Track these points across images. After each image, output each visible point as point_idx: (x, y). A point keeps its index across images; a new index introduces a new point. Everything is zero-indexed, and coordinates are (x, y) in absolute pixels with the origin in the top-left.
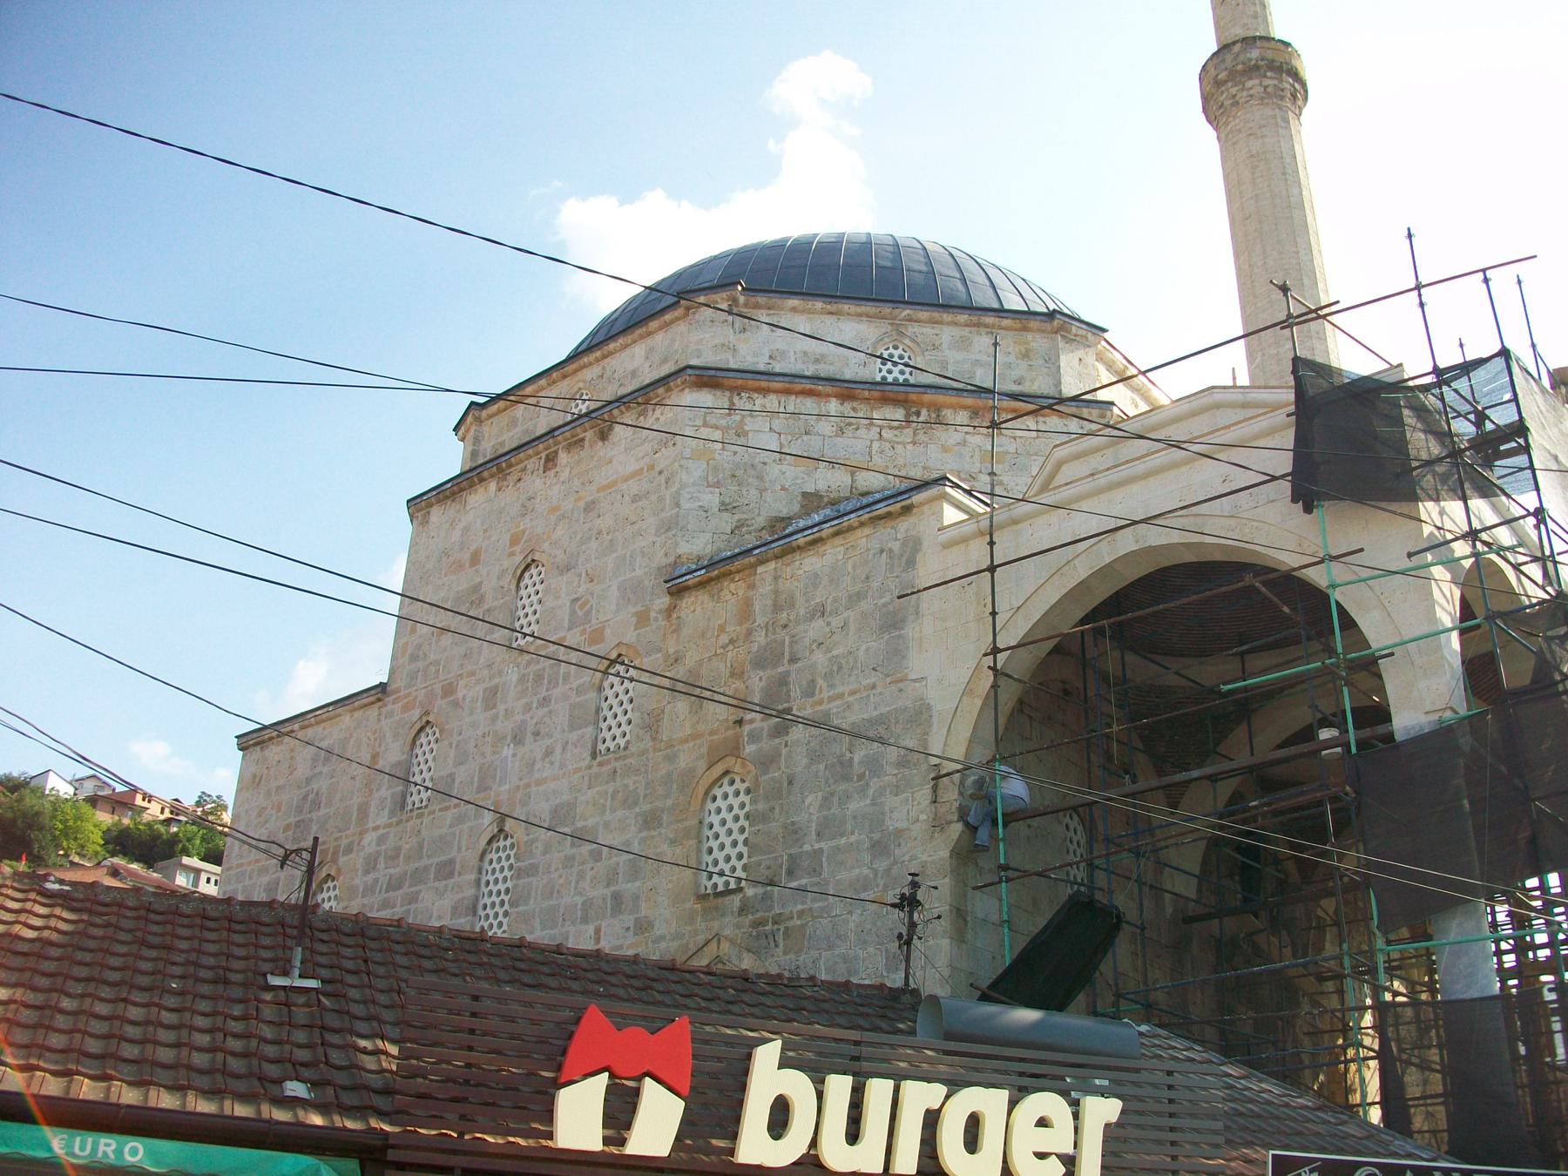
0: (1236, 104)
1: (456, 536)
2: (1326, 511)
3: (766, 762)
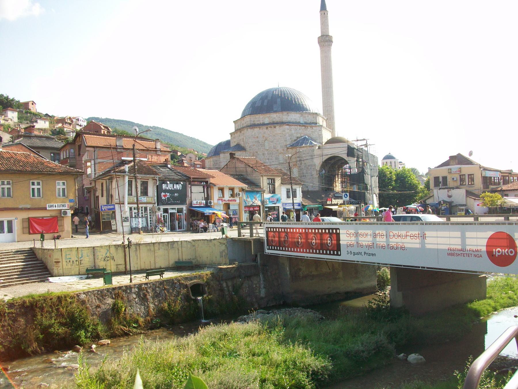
0: (324, 46)
1: (253, 133)
2: (349, 157)
3: (299, 167)
